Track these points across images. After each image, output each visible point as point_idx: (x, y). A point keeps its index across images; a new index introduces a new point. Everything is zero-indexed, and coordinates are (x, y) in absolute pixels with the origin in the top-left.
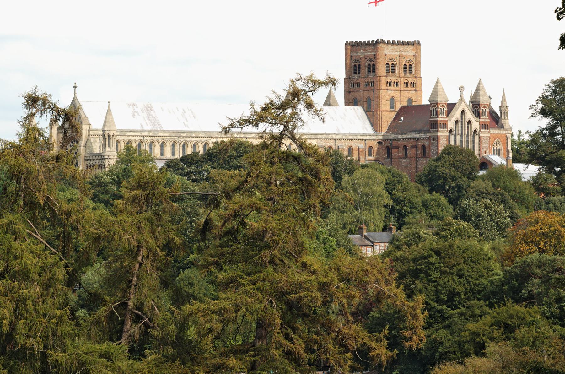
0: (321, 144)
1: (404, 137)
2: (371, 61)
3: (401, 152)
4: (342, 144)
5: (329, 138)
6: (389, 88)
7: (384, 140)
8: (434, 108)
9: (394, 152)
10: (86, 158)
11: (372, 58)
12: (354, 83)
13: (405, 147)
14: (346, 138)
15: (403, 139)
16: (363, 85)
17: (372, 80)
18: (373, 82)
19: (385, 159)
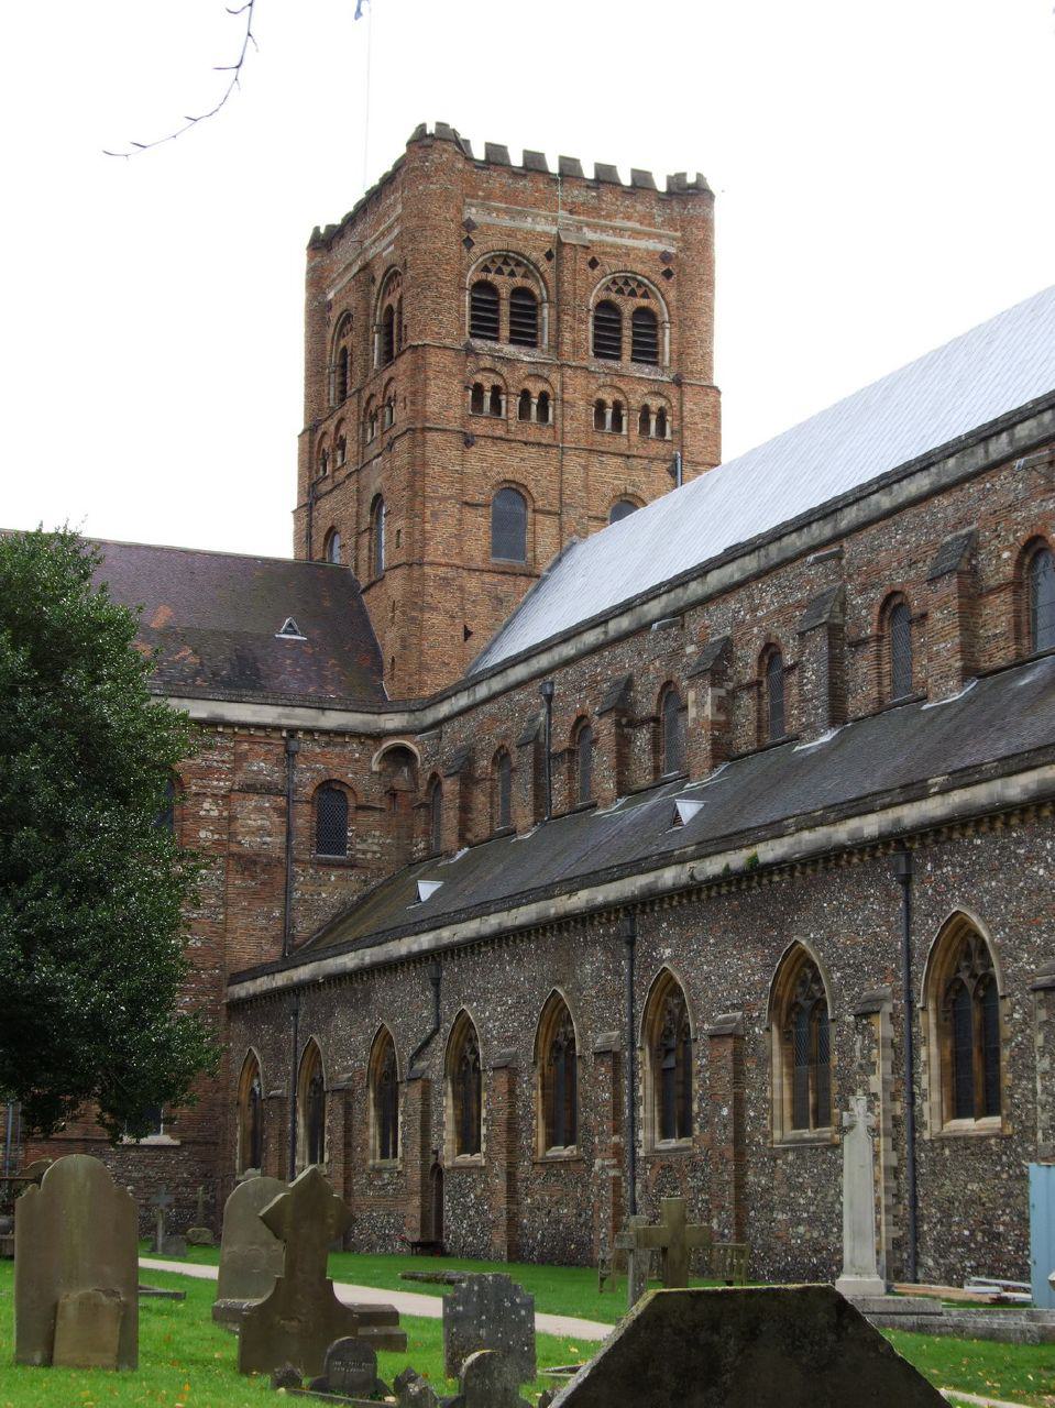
2: (627, 283)
11: (649, 270)
16: (576, 419)
17: (655, 403)
18: (662, 414)
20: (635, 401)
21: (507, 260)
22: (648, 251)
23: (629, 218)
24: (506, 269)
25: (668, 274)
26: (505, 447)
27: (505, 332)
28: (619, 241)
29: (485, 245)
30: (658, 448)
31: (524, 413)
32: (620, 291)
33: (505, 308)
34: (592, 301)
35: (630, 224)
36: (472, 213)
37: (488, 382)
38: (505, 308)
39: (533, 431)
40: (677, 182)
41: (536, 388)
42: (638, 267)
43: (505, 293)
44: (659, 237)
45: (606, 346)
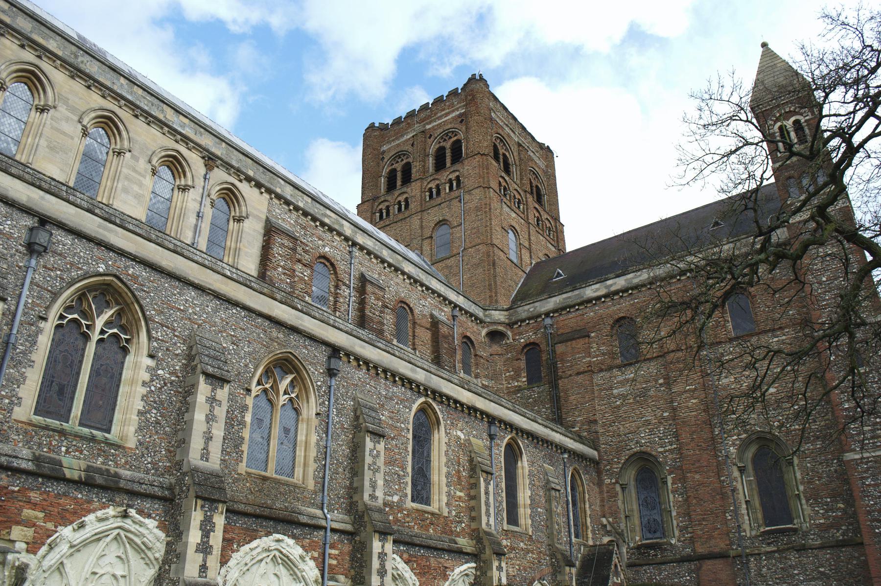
0: (287, 227)
1: (613, 289)
2: (447, 135)
4: (376, 276)
5: (327, 221)
6: (505, 200)
7: (510, 325)
8: (789, 123)
12: (388, 208)
14: (391, 261)
18: (458, 178)
19: (519, 389)
21: (399, 155)
22: (452, 118)
23: (444, 110)
24: (399, 160)
25: (461, 122)
26: (388, 228)
27: (399, 183)
28: (440, 121)
32: (445, 140)
35: (443, 113)
36: (385, 148)
39: (401, 216)
42: (449, 126)
43: (399, 169)
44: (457, 109)
45: (440, 165)
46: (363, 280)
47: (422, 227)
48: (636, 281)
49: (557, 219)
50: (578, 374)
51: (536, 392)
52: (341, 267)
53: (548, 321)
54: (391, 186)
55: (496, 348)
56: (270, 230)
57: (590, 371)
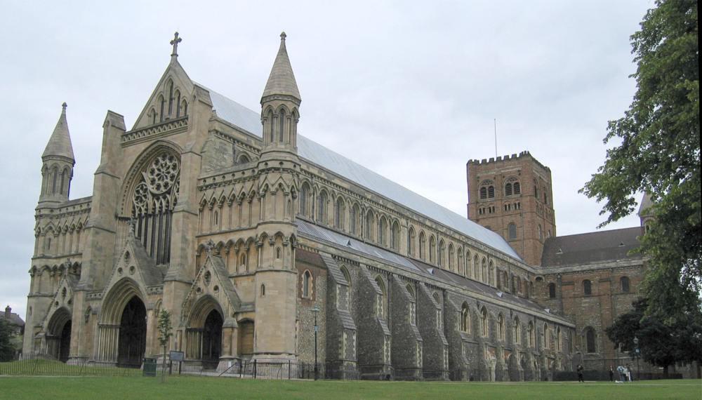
2: (512, 179)
3: (579, 289)
7: (544, 275)
9: (567, 291)
10: (202, 183)
12: (484, 209)
13: (587, 284)
15: (583, 271)
18: (519, 204)
19: (547, 300)
20: (512, 203)
21: (486, 182)
27: (488, 196)
29: (481, 181)
30: (519, 211)
31: (490, 212)
33: (487, 192)
34: (504, 185)
36: (479, 175)
37: (482, 208)
38: (487, 192)
39: (491, 215)
40: (522, 155)
41: (491, 206)
43: (487, 188)
45: (509, 192)
46: (513, 277)
47: (503, 224)
48: (592, 268)
49: (552, 209)
50: (570, 298)
51: (554, 301)
52: (508, 272)
53: (559, 277)
54: (483, 196)
55: (538, 283)
56: (498, 271)
57: (575, 297)
